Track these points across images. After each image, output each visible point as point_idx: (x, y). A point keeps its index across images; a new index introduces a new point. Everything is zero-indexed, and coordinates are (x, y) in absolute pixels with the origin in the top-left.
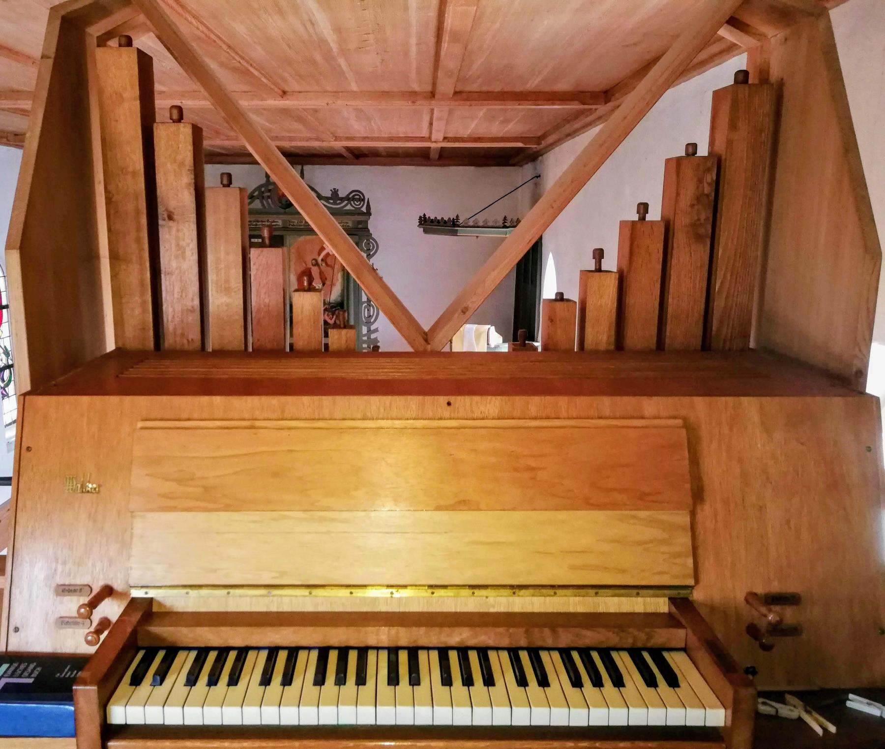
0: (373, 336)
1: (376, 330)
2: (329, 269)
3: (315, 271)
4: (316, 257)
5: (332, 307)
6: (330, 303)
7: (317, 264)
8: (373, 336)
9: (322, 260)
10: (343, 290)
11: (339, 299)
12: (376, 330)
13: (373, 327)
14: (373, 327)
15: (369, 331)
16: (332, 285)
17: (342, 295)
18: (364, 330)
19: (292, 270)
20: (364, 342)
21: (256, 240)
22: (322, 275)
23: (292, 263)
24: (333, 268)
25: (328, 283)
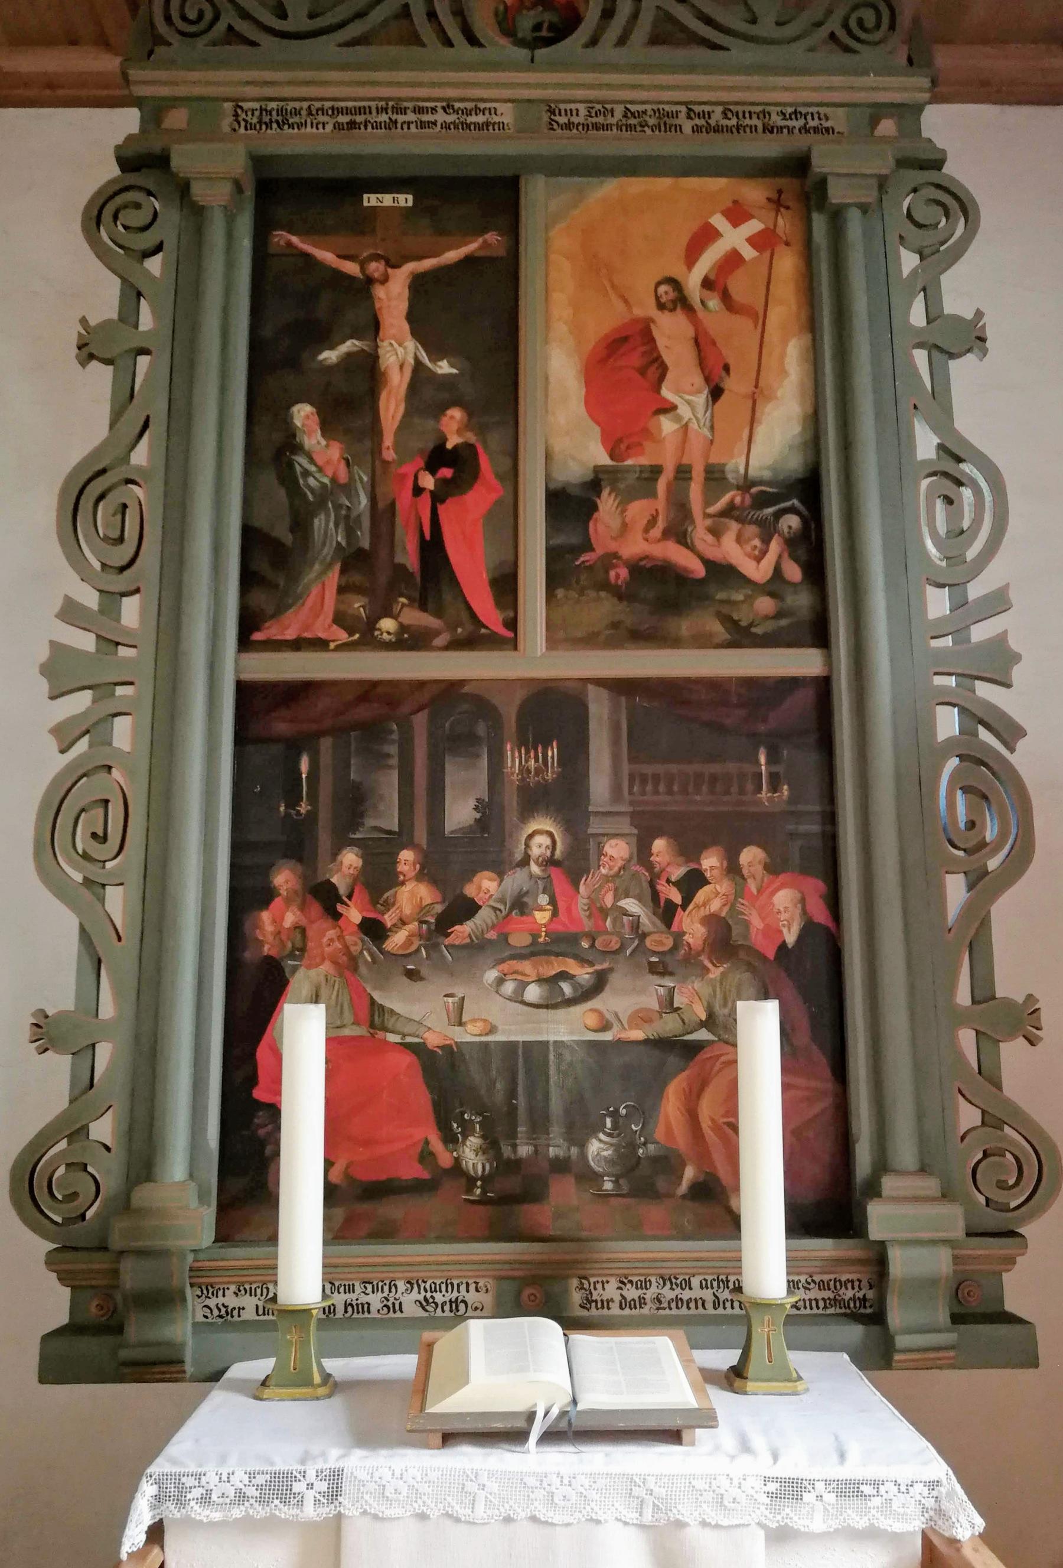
0: (979, 633)
1: (998, 602)
2: (742, 324)
3: (672, 334)
4: (677, 270)
5: (762, 501)
6: (746, 484)
7: (681, 302)
8: (979, 633)
9: (707, 284)
10: (814, 419)
11: (795, 465)
12: (998, 602)
13: (975, 590)
14: (975, 590)
15: (959, 604)
16: (756, 398)
17: (814, 442)
18: (938, 603)
19: (560, 329)
20: (941, 665)
21: (387, 200)
22: (702, 345)
23: (560, 299)
24: (760, 319)
25: (735, 385)
